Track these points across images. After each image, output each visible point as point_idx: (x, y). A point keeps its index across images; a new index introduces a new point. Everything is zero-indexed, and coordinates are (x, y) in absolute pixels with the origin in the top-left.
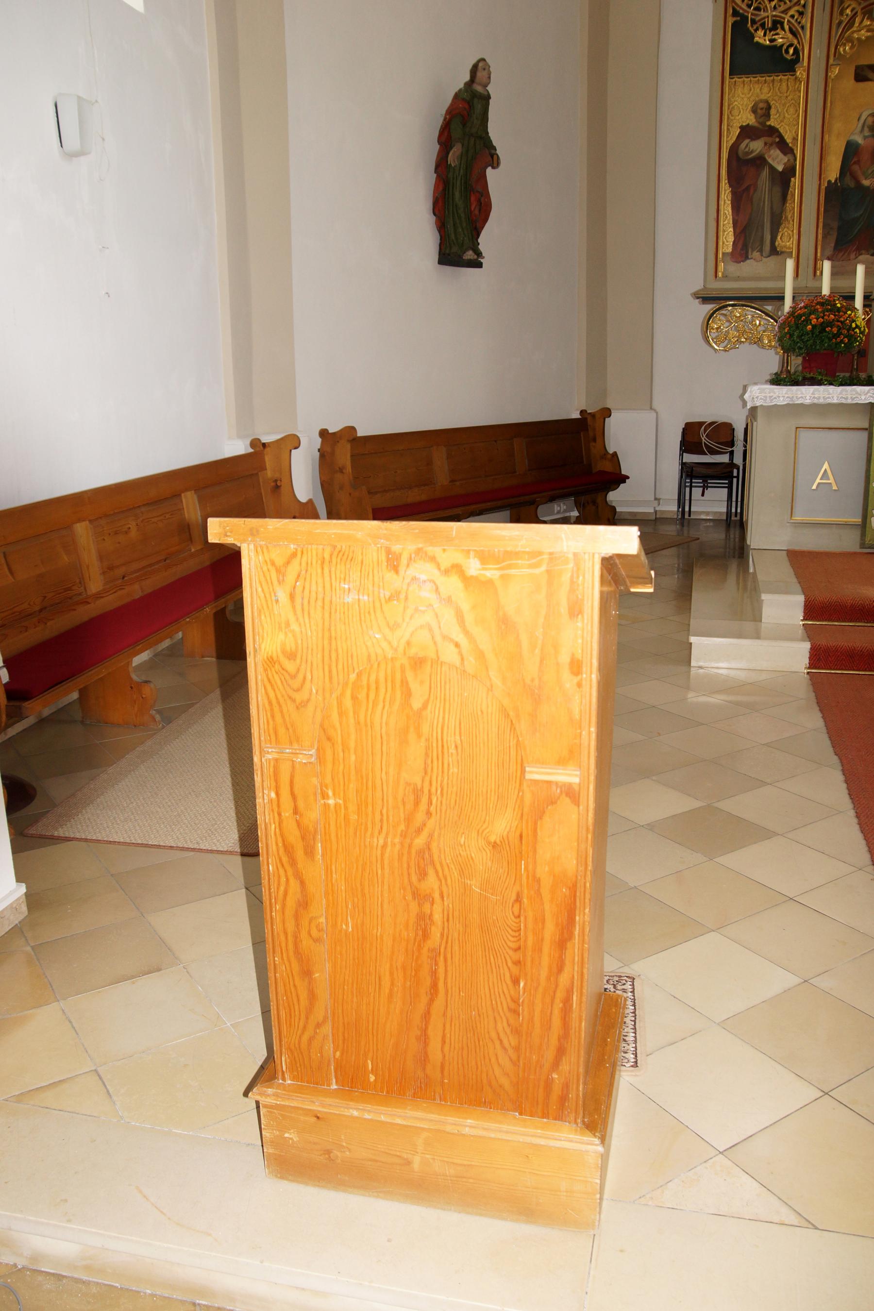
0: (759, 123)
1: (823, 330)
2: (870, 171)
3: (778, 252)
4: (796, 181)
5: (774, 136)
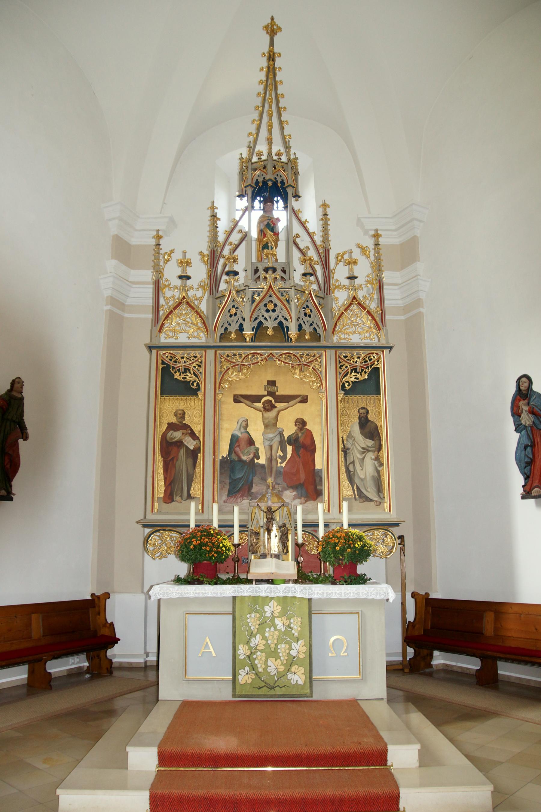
0: (178, 422)
1: (201, 549)
2: (246, 451)
3: (192, 497)
4: (200, 456)
5: (187, 430)
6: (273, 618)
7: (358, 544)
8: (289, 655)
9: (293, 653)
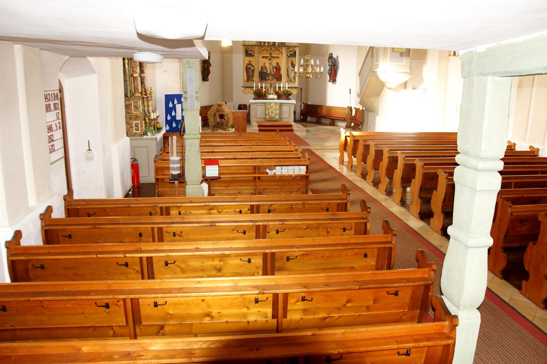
6: (273, 106)
7: (289, 93)
8: (276, 113)
9: (277, 113)
